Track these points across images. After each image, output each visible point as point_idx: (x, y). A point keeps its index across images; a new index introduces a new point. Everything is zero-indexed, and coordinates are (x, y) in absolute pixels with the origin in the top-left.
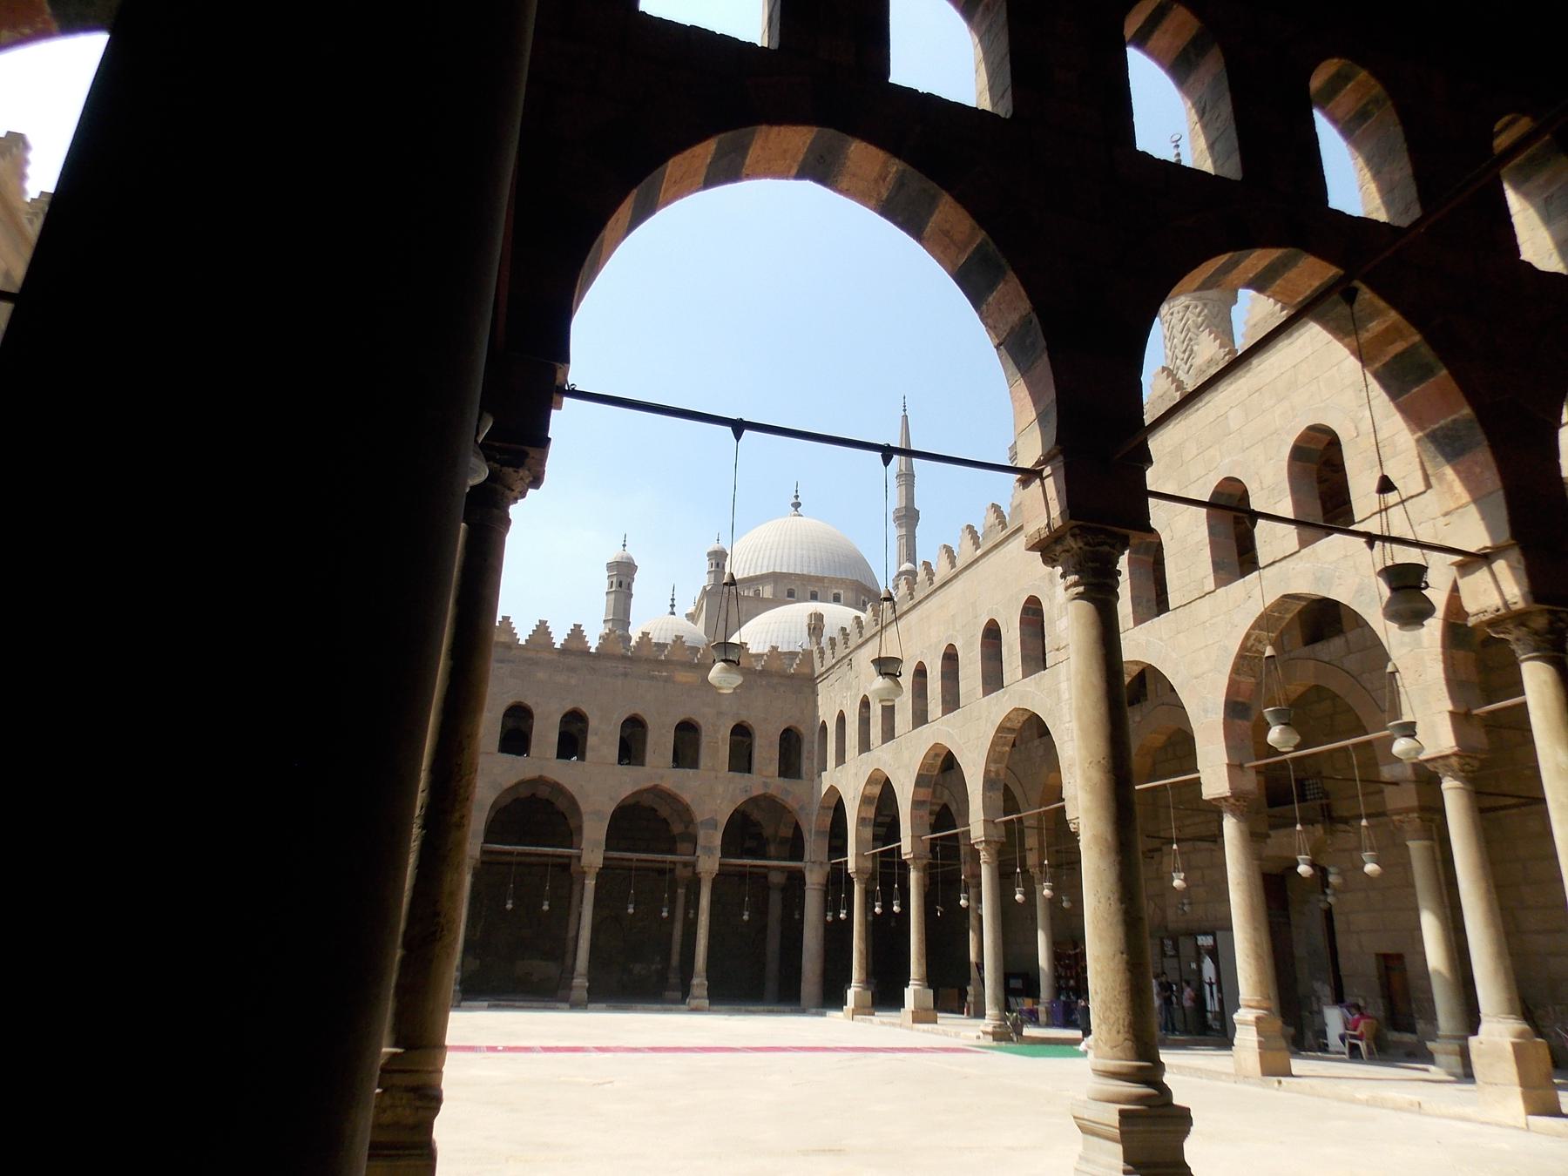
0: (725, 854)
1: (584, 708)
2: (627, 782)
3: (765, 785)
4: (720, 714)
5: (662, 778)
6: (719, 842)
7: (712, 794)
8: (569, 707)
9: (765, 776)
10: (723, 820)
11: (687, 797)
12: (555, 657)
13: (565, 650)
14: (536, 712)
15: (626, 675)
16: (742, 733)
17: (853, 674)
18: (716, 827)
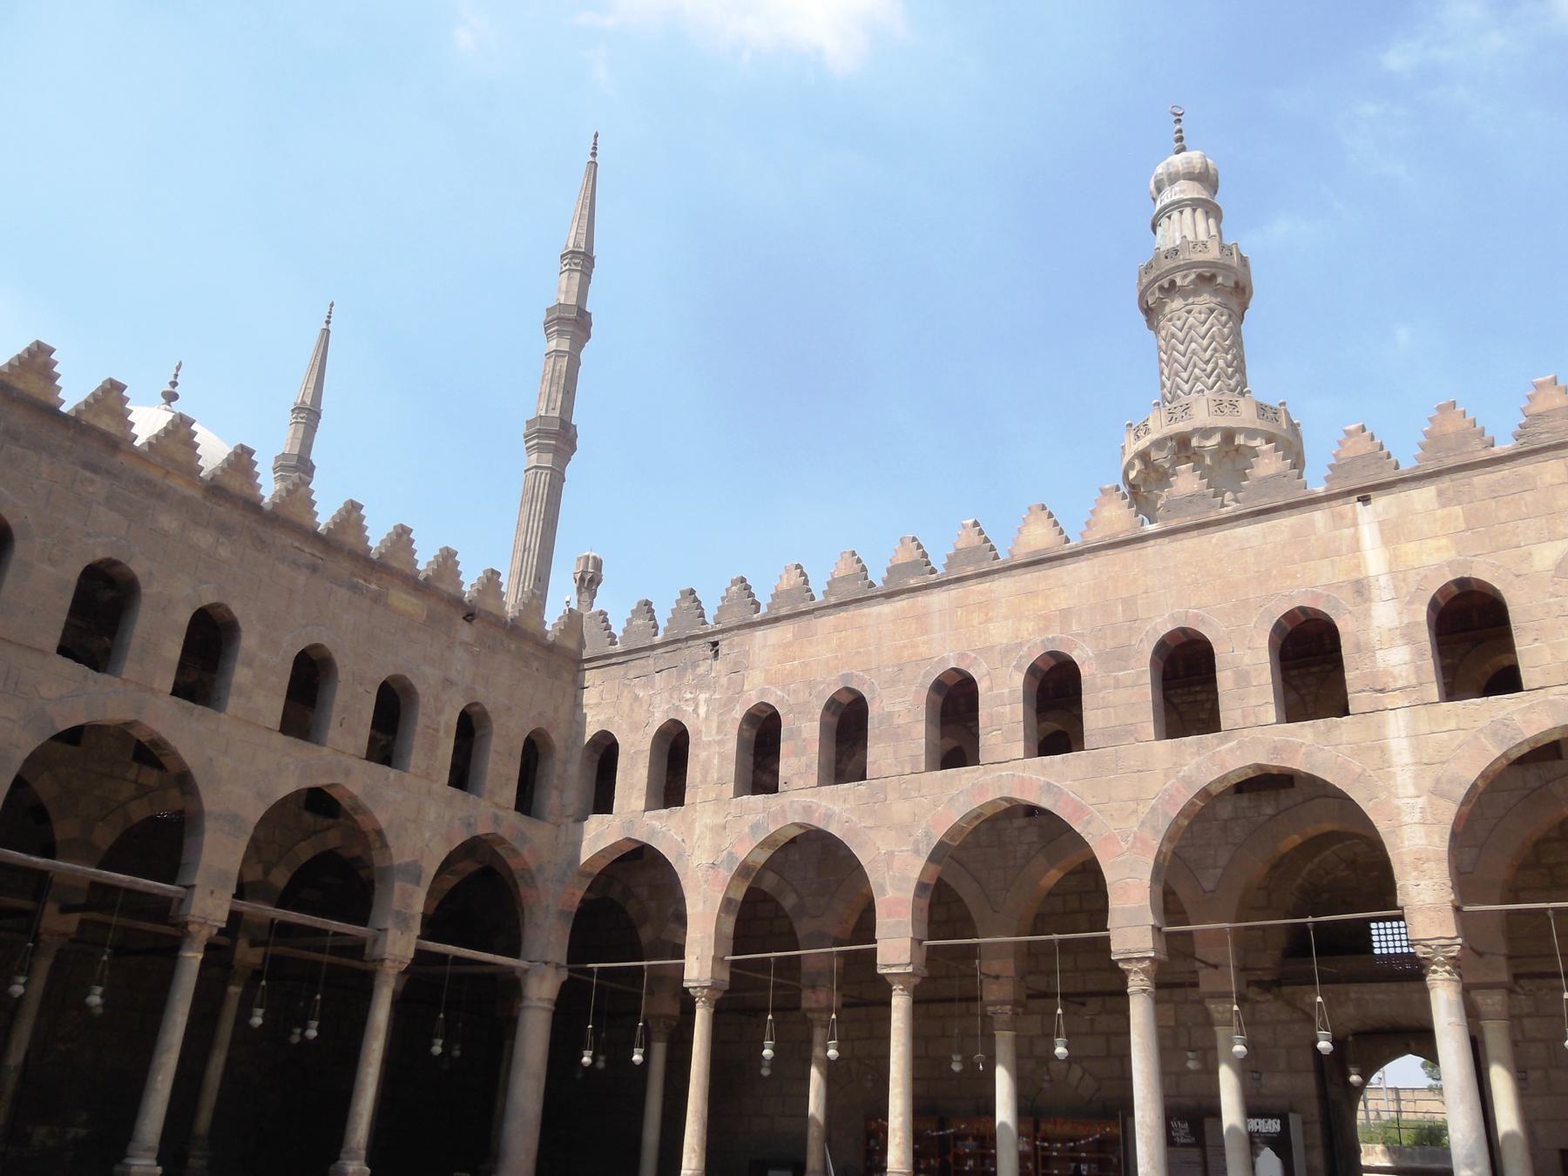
0: (424, 936)
1: (237, 610)
2: (290, 769)
3: (496, 819)
4: (448, 682)
5: (347, 773)
6: (418, 905)
7: (418, 822)
8: (208, 598)
9: (491, 808)
10: (431, 868)
11: (382, 818)
12: (196, 494)
13: (215, 489)
14: (148, 590)
15: (314, 569)
16: (470, 728)
17: (718, 665)
18: (417, 880)
